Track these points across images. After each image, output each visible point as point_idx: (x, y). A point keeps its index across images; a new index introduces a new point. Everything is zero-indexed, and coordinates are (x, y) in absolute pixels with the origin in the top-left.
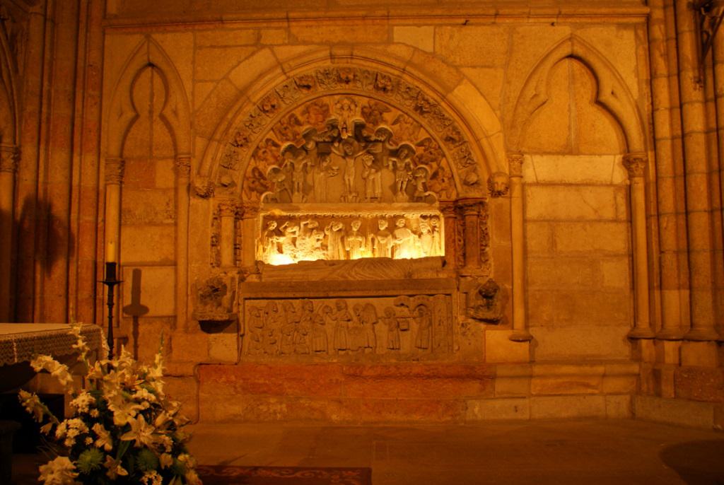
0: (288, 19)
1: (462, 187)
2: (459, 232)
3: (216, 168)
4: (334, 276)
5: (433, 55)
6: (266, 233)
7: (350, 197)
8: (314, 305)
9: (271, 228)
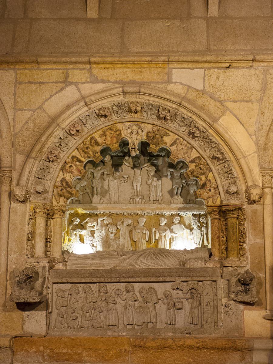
0: (90, 62)
1: (225, 196)
2: (222, 230)
3: (32, 178)
4: (124, 264)
5: (203, 92)
6: (71, 227)
7: (137, 200)
8: (108, 288)
9: (75, 223)
